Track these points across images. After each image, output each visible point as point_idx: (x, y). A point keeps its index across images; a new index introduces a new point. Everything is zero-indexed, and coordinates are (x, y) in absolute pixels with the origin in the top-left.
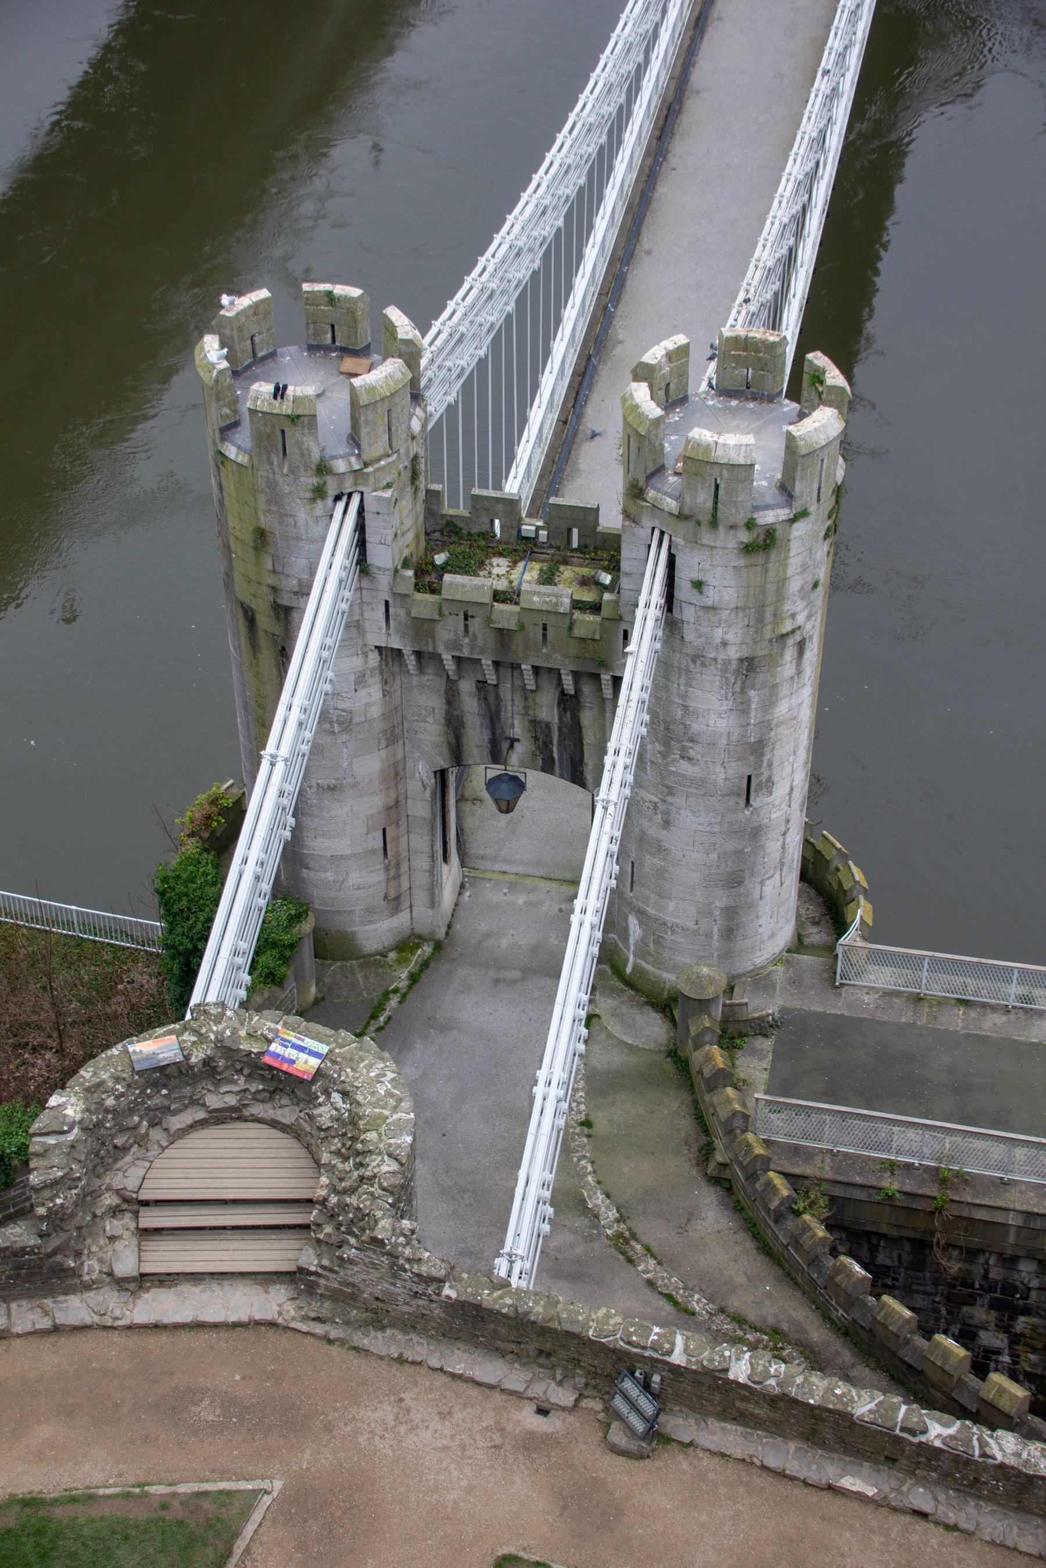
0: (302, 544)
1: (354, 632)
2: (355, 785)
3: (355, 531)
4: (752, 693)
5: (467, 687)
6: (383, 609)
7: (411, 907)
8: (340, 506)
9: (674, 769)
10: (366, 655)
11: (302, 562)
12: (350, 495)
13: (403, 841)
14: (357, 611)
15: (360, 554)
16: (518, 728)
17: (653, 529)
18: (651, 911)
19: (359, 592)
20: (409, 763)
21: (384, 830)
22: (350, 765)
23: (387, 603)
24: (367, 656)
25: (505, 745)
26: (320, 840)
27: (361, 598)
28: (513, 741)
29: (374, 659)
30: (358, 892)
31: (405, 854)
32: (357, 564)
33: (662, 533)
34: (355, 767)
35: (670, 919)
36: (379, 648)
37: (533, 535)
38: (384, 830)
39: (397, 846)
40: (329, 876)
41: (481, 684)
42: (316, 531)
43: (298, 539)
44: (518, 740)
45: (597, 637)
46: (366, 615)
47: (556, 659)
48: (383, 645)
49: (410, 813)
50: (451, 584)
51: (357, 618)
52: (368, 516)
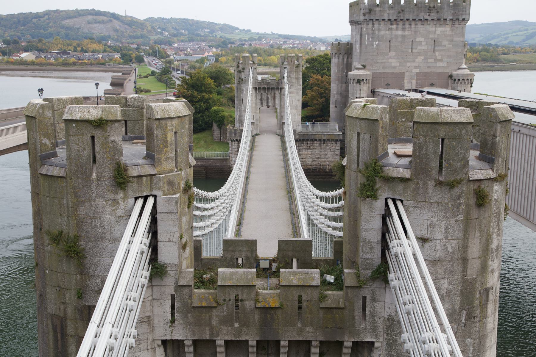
0: (106, 243)
1: (145, 325)
3: (149, 232)
4: (469, 340)
6: (169, 304)
8: (140, 202)
10: (154, 350)
11: (106, 261)
12: (146, 198)
14: (149, 308)
15: (152, 254)
17: (386, 200)
19: (150, 290)
23: (173, 297)
24: (155, 351)
27: (152, 295)
32: (149, 264)
33: (394, 201)
36: (165, 343)
37: (268, 266)
42: (117, 229)
43: (103, 239)
45: (342, 306)
46: (157, 311)
47: (309, 332)
48: (168, 338)
50: (223, 273)
51: (148, 314)
52: (159, 217)
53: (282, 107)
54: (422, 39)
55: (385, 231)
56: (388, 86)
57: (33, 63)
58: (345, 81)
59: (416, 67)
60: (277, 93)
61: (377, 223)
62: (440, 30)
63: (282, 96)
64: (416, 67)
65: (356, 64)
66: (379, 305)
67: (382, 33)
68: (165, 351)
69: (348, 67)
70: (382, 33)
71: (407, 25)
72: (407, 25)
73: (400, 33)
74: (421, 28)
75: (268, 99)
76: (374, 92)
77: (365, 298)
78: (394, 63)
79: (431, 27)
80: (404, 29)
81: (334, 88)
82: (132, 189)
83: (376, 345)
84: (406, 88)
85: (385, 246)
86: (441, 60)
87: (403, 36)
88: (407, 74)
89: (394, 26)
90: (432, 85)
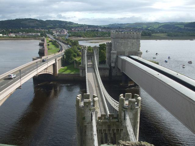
5: (104, 134)
16: (109, 139)
25: (107, 141)
28: (108, 140)
41: (105, 134)
53: (94, 60)
54: (129, 43)
55: (125, 115)
56: (121, 55)
57: (14, 37)
58: (110, 53)
59: (128, 50)
60: (92, 57)
61: (124, 114)
62: (134, 41)
64: (128, 50)
65: (113, 49)
66: (124, 124)
67: (119, 41)
69: (111, 50)
70: (119, 41)
71: (126, 40)
72: (126, 40)
73: (124, 41)
74: (129, 40)
75: (90, 58)
76: (117, 56)
78: (123, 49)
79: (131, 40)
80: (125, 40)
81: (107, 55)
82: (92, 110)
84: (126, 55)
85: (125, 117)
86: (134, 48)
87: (125, 42)
88: (126, 52)
89: (122, 40)
90: (132, 55)
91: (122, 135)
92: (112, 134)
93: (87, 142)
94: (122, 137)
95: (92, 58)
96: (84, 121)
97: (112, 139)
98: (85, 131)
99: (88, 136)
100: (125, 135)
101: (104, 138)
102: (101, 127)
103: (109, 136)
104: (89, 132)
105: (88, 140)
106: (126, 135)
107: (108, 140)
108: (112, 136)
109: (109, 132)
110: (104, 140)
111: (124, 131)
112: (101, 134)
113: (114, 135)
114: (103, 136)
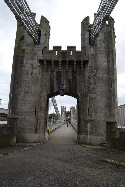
2: (31, 92)
5: (55, 73)
7: (39, 133)
9: (97, 77)
13: (39, 112)
18: (93, 119)
20: (42, 93)
21: (36, 107)
22: (31, 87)
23: (43, 50)
26: (22, 106)
28: (63, 85)
29: (39, 63)
30: (29, 123)
31: (39, 117)
34: (32, 87)
35: (98, 119)
38: (36, 107)
39: (38, 113)
40: (23, 117)
41: (57, 73)
44: (64, 85)
49: (41, 107)
63: (71, 115)
68: (40, 64)
77: (86, 50)
83: (89, 61)
91: (87, 74)
92: (70, 74)
93: (22, 79)
94: (87, 77)
95: (69, 115)
96: (23, 42)
97: (69, 83)
98: (22, 60)
99: (26, 67)
100: (93, 72)
101: (55, 81)
102: (50, 55)
103: (65, 77)
104: (29, 61)
105: (25, 75)
106: (94, 70)
107: (63, 85)
108: (70, 77)
109: (65, 71)
110: (56, 90)
111: (90, 64)
112: (50, 73)
113: (73, 75)
114: (53, 77)
